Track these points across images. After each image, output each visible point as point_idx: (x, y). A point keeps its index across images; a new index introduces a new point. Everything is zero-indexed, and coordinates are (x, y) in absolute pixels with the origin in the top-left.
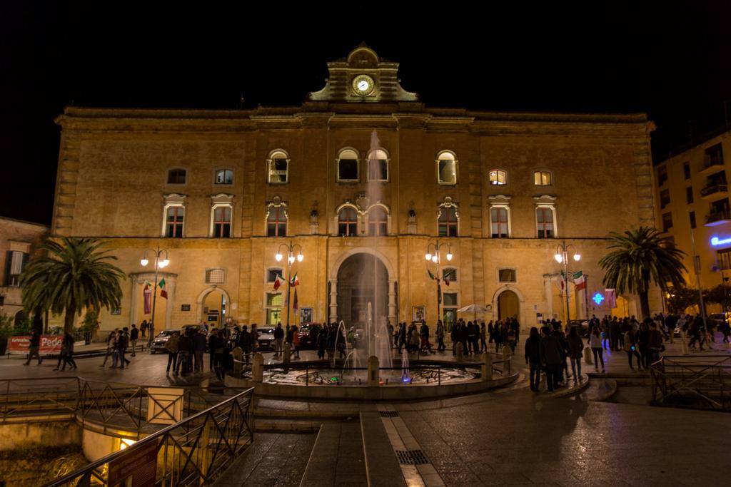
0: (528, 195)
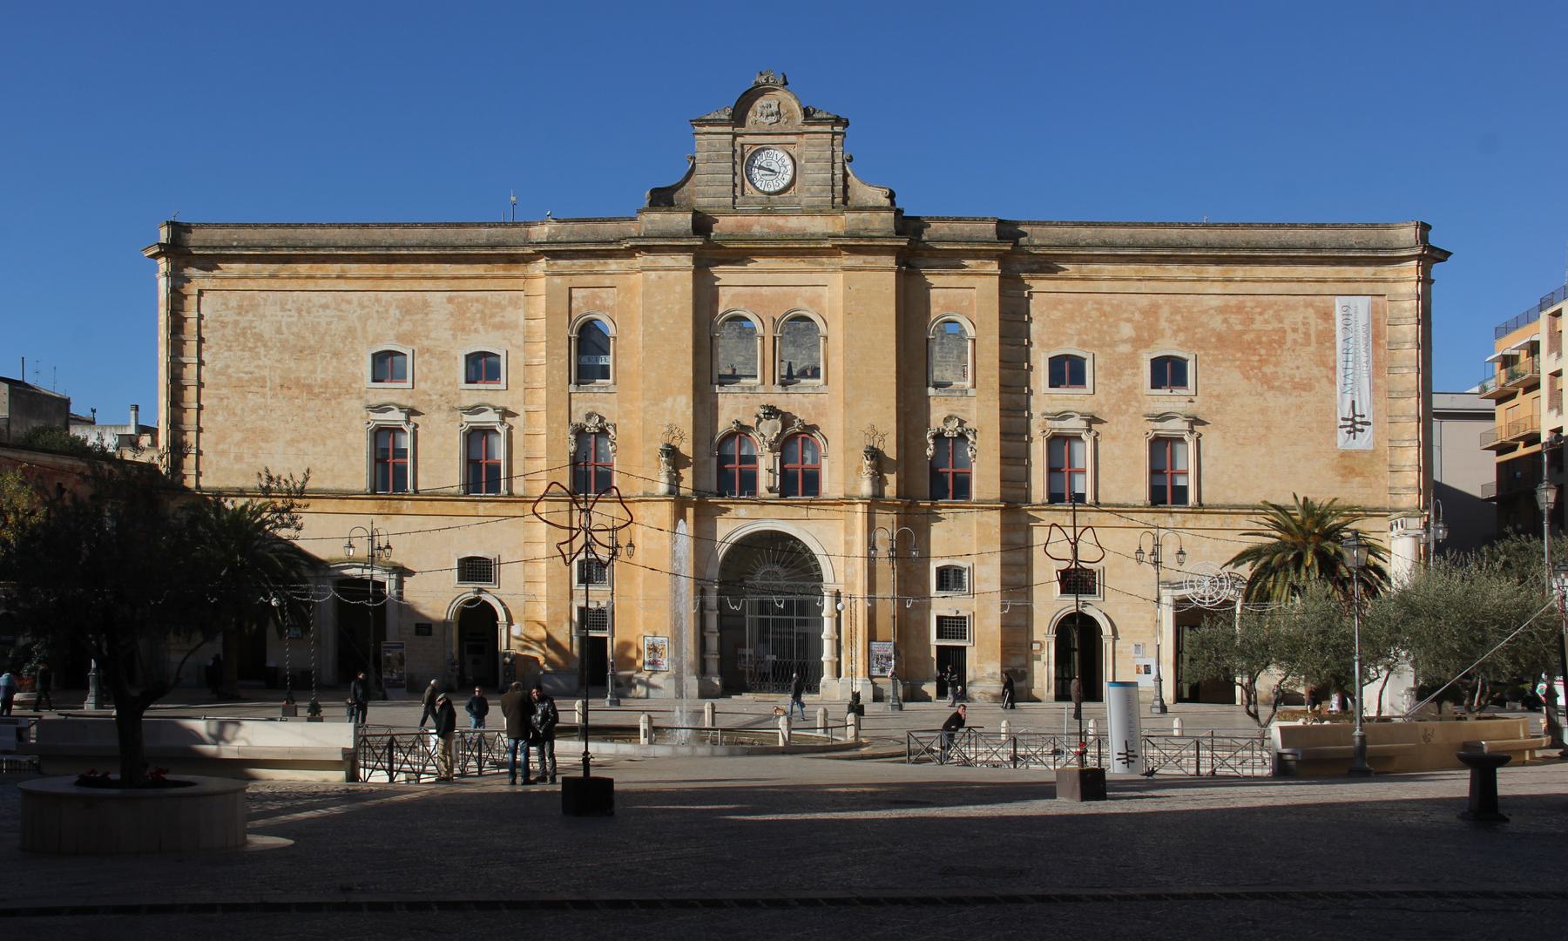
0: (1132, 410)
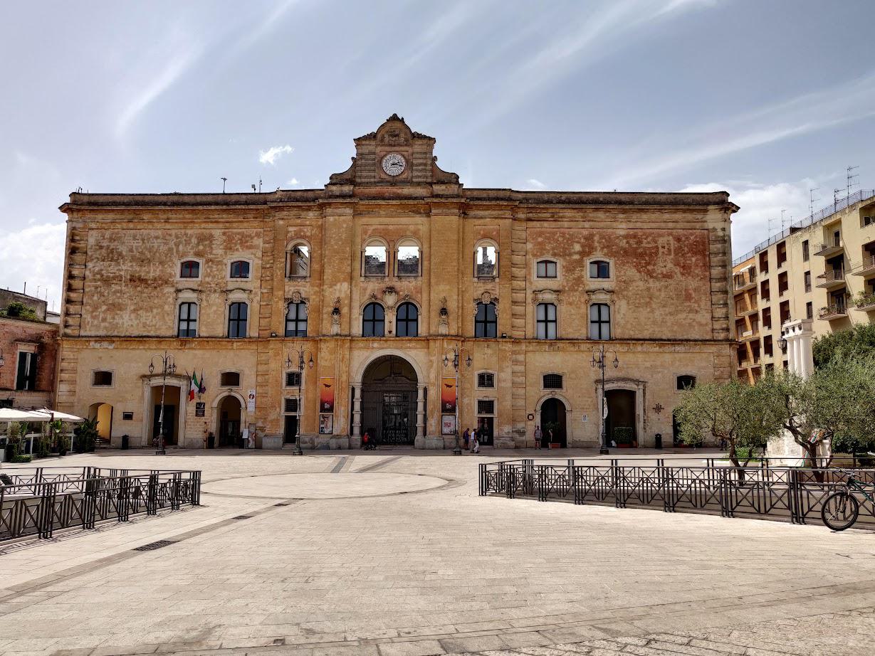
0: (580, 289)
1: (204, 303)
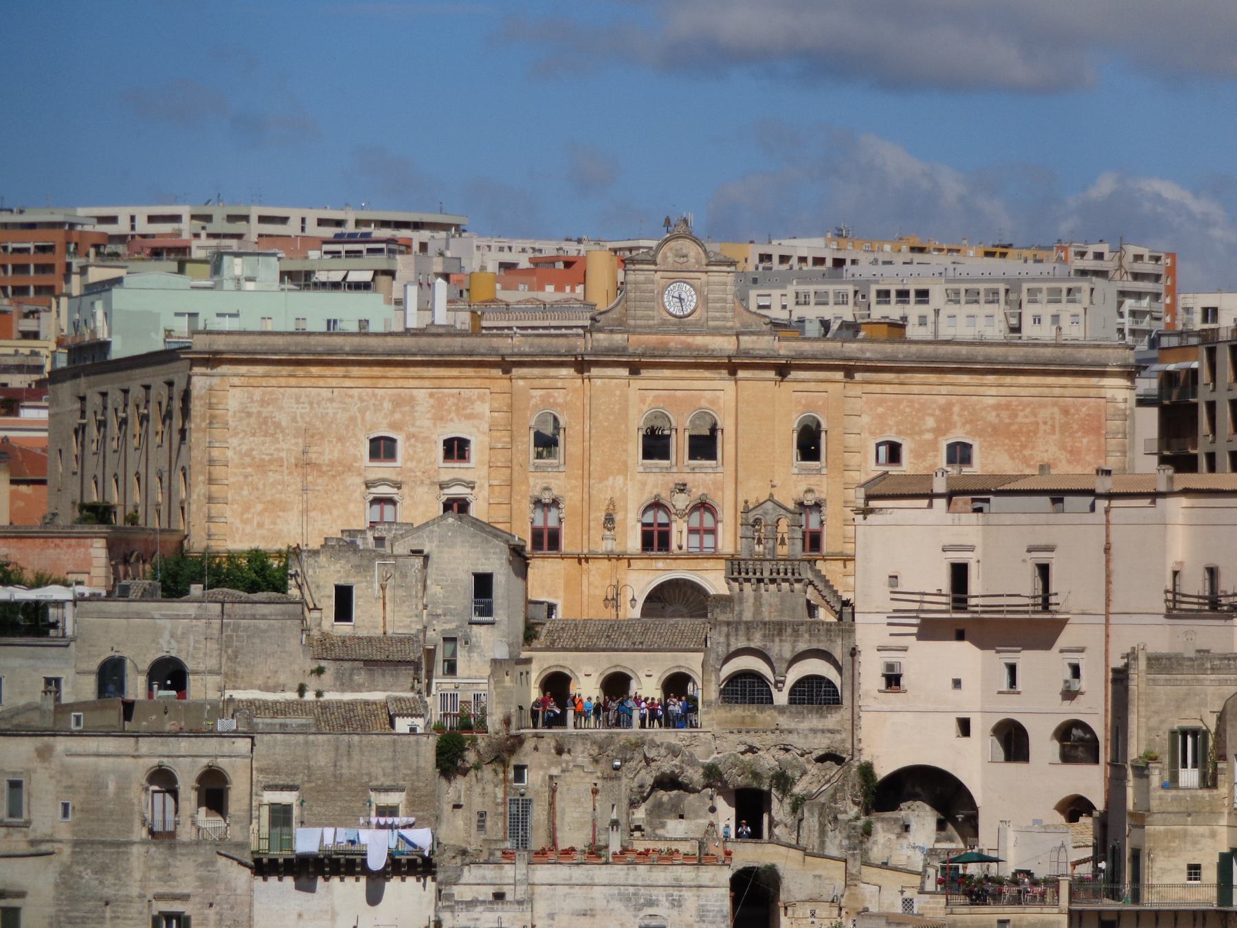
1: (407, 501)
